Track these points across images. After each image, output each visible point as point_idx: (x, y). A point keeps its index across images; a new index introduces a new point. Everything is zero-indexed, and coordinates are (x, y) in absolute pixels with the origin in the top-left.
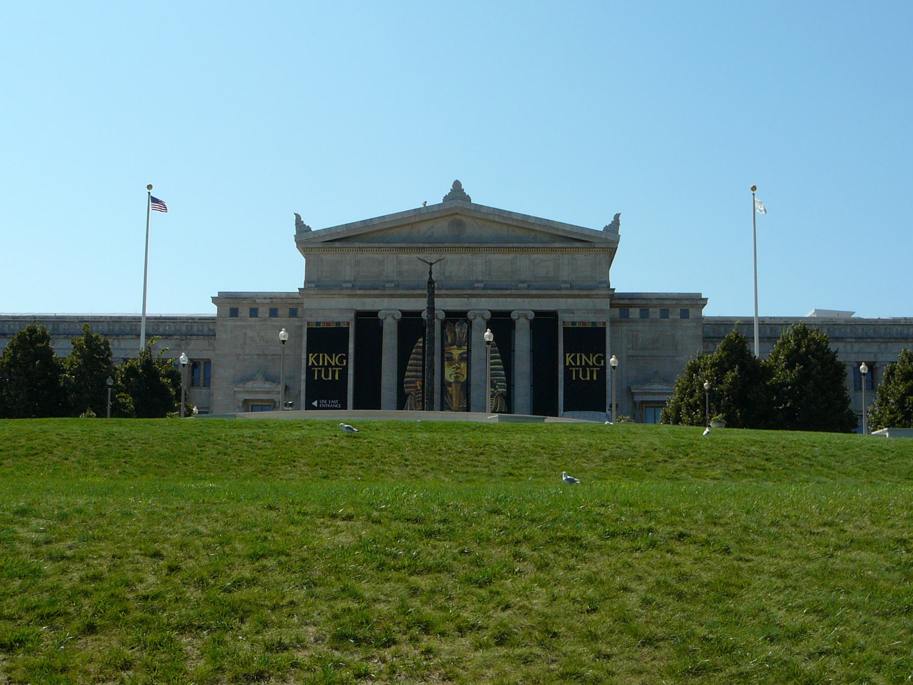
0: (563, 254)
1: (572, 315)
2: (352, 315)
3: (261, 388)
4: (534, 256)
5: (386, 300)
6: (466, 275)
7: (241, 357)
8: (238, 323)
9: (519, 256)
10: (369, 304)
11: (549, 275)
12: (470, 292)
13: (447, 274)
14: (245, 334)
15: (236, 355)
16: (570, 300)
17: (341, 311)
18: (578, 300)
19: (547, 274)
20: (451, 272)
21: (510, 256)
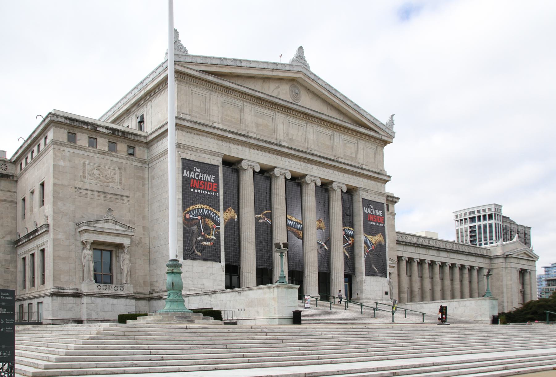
0: (360, 139)
1: (367, 193)
2: (221, 160)
3: (112, 229)
4: (344, 137)
5: (247, 150)
6: (303, 141)
7: (81, 191)
8: (77, 151)
9: (335, 133)
10: (235, 151)
11: (352, 156)
12: (310, 157)
13: (290, 137)
14: (84, 165)
15: (76, 188)
16: (365, 180)
17: (212, 153)
18: (370, 182)
19: (352, 153)
20: (293, 135)
21: (329, 132)
